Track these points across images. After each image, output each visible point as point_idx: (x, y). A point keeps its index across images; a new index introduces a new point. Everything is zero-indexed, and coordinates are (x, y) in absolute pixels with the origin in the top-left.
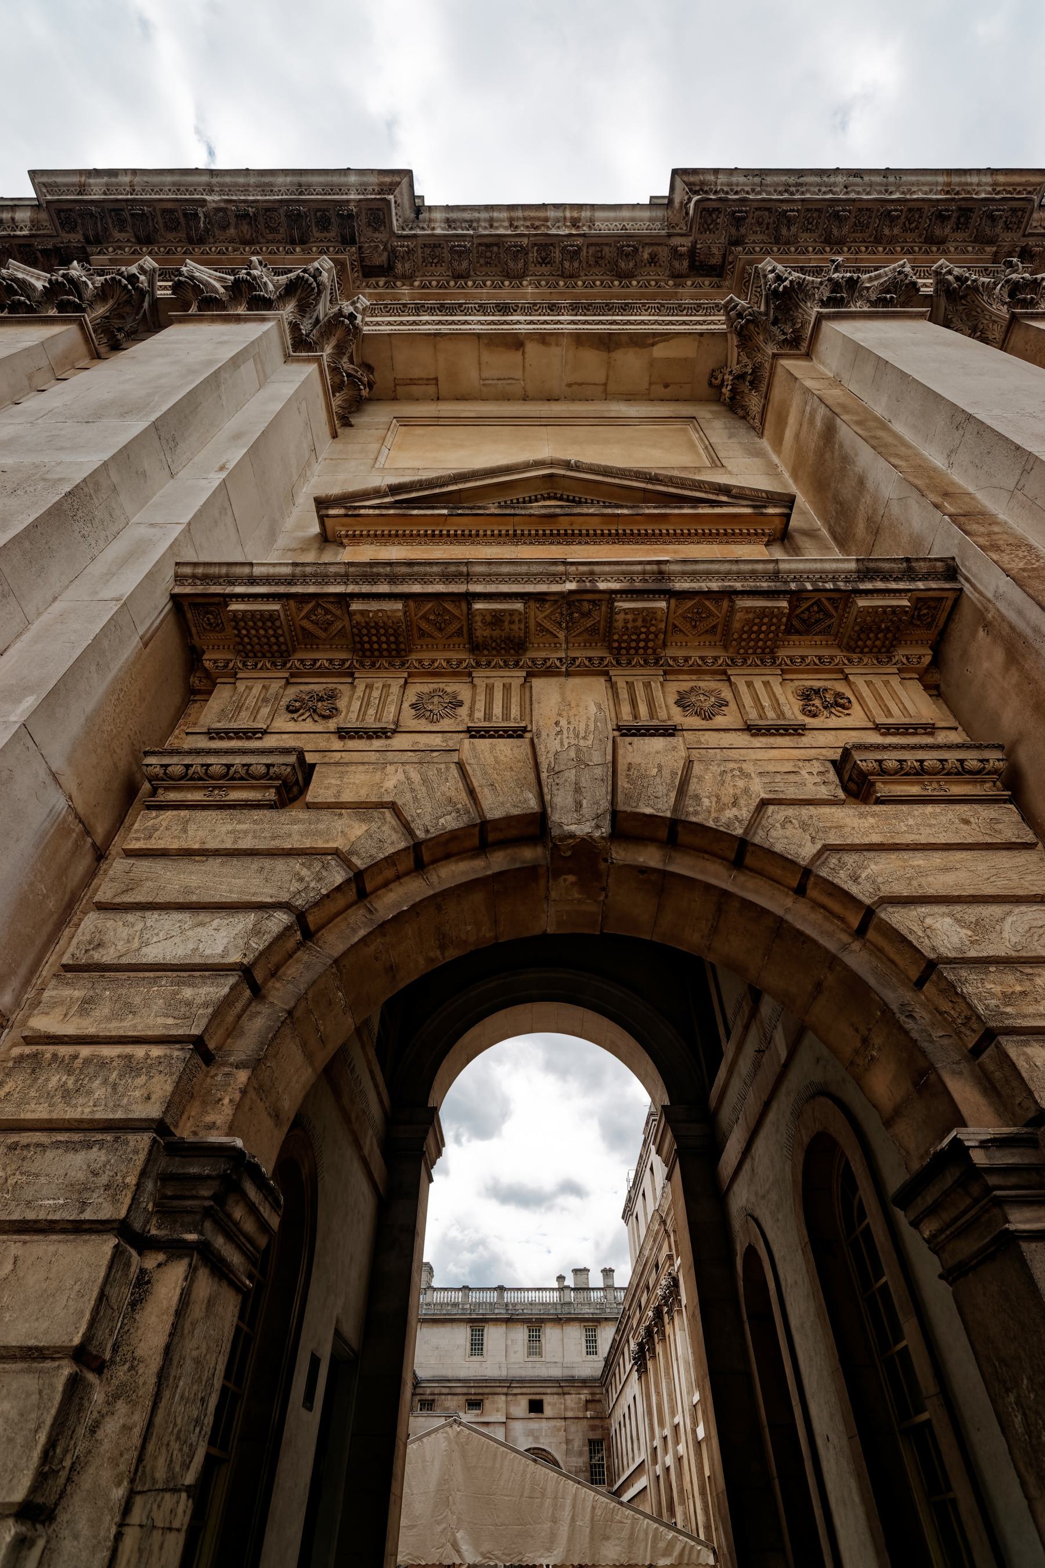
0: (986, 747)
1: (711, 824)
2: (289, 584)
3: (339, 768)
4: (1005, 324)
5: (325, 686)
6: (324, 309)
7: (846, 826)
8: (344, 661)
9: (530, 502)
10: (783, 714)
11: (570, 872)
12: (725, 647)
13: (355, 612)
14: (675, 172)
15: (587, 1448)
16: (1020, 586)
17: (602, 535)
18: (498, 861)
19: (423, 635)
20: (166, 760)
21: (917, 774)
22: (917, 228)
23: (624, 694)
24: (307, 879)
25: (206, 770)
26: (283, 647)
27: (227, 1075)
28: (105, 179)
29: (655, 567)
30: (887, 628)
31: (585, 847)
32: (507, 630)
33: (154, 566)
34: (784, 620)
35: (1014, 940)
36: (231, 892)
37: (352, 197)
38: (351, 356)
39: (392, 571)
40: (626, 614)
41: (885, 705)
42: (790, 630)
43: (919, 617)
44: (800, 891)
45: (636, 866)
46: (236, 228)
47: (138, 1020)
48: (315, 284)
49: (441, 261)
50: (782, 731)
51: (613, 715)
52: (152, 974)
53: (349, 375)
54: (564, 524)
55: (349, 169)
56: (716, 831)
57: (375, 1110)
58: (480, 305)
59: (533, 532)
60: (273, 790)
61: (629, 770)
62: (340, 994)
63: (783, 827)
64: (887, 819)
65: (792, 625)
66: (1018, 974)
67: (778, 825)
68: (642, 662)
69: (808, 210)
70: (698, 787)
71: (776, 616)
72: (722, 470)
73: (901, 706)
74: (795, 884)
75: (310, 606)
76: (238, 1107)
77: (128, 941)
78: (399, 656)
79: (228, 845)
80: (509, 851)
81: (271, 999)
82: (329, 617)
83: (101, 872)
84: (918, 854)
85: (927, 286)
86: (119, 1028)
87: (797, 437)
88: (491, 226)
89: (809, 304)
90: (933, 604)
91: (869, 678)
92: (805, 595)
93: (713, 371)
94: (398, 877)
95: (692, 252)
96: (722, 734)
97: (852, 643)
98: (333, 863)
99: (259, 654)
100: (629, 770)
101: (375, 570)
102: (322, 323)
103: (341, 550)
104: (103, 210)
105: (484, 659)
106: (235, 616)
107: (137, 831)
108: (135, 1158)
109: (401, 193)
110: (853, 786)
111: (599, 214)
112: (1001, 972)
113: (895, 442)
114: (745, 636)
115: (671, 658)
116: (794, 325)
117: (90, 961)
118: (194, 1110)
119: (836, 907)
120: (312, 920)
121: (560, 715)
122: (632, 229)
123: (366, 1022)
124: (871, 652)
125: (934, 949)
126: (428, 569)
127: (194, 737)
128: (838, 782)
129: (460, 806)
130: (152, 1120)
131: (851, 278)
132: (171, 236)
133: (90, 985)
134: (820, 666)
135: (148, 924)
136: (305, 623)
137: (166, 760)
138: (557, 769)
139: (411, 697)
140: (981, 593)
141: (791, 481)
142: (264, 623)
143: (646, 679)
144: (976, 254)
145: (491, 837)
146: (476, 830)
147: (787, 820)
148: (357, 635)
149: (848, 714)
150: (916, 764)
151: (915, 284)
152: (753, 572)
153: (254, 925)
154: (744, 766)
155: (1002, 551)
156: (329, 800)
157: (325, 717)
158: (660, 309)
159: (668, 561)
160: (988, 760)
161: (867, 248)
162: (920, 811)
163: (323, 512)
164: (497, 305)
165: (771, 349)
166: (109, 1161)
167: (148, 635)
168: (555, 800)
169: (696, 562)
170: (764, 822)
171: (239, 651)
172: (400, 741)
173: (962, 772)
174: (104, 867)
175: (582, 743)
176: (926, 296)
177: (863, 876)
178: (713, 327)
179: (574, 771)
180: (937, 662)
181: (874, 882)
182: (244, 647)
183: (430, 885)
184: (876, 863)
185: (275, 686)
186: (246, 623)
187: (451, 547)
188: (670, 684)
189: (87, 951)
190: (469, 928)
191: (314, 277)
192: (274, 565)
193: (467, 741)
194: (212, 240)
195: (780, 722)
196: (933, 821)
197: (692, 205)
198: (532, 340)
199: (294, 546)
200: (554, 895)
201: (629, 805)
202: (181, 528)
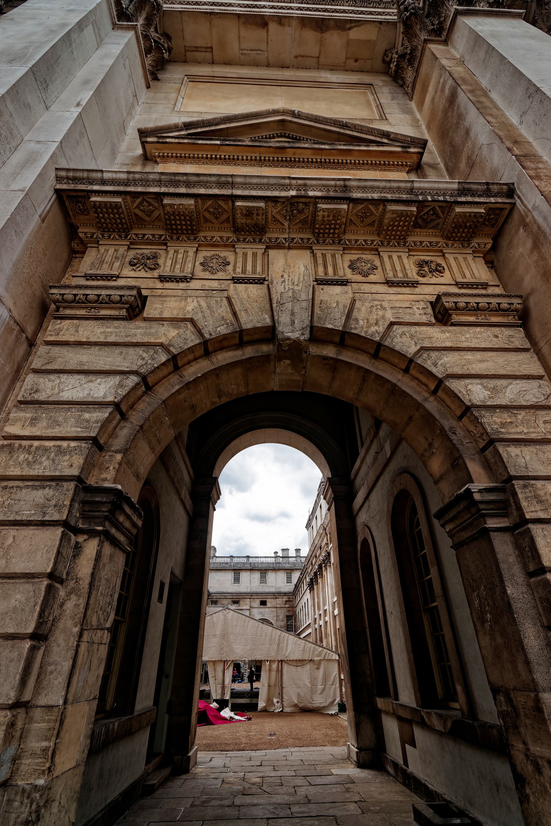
0: (513, 296)
1: (363, 334)
2: (126, 185)
3: (161, 299)
5: (151, 250)
8: (161, 236)
10: (407, 274)
12: (379, 235)
13: (167, 205)
18: (249, 352)
19: (207, 222)
20: (63, 291)
21: (475, 310)
23: (320, 261)
24: (146, 359)
30: (470, 226)
31: (296, 343)
32: (255, 219)
34: (413, 218)
35: (511, 397)
36: (105, 365)
40: (324, 212)
41: (463, 272)
42: (416, 225)
44: (406, 371)
45: (322, 356)
50: (405, 285)
52: (67, 406)
60: (124, 310)
62: (167, 418)
63: (401, 337)
64: (455, 334)
65: (417, 222)
66: (510, 413)
67: (398, 336)
68: (331, 242)
74: (404, 367)
76: (118, 471)
77: (52, 389)
79: (102, 339)
80: (255, 347)
82: (151, 207)
83: (33, 353)
84: (469, 353)
90: (497, 212)
91: (455, 255)
92: (427, 204)
94: (195, 359)
96: (373, 285)
97: (449, 235)
98: (160, 350)
99: (111, 230)
101: (177, 178)
107: (50, 331)
110: (440, 316)
113: (491, 106)
114: (390, 228)
115: (348, 240)
116: (440, 18)
118: (96, 472)
119: (424, 379)
120: (150, 380)
121: (284, 271)
124: (459, 240)
125: (470, 401)
126: (209, 179)
127: (78, 278)
128: (432, 314)
129: (228, 321)
130: (75, 476)
133: (34, 411)
134: (431, 248)
136: (137, 211)
137: (63, 291)
138: (282, 302)
139: (200, 259)
140: (525, 206)
142: (112, 210)
143: (333, 252)
145: (246, 338)
146: (237, 335)
147: (403, 333)
148: (168, 220)
149: (442, 276)
152: (399, 188)
154: (383, 303)
155: (542, 180)
156: (156, 316)
157: (151, 269)
159: (350, 179)
160: (513, 304)
162: (474, 330)
165: (423, 36)
166: (55, 494)
168: (280, 319)
169: (366, 180)
170: (391, 334)
172: (194, 284)
173: (499, 310)
175: (296, 288)
177: (440, 363)
179: (291, 303)
180: (495, 248)
182: (102, 225)
183: (213, 363)
184: (447, 357)
185: (122, 250)
186: (102, 210)
189: (30, 394)
190: (233, 387)
192: (116, 172)
193: (232, 285)
195: (405, 279)
196: (479, 336)
200: (278, 370)
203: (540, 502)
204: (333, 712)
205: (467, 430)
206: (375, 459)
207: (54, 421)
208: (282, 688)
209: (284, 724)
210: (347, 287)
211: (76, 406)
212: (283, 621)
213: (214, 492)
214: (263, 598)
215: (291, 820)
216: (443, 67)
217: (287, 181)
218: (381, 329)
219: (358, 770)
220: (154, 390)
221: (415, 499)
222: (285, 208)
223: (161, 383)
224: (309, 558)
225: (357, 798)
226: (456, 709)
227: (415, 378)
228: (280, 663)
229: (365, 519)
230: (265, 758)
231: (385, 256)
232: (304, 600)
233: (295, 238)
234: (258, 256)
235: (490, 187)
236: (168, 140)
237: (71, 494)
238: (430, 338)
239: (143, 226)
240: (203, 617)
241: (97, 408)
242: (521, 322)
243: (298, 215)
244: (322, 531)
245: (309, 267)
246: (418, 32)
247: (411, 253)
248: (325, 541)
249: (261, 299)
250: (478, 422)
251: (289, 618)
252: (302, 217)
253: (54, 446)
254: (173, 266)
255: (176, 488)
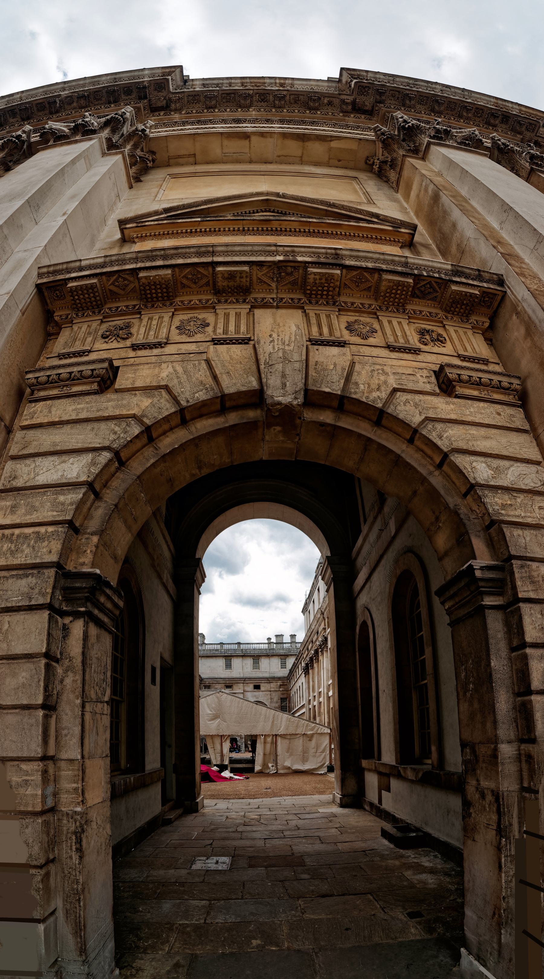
0: (513, 377)
1: (364, 400)
2: (102, 267)
3: (134, 368)
4: (528, 171)
5: (124, 321)
6: (126, 129)
7: (438, 408)
8: (135, 306)
9: (254, 213)
10: (408, 341)
11: (277, 425)
12: (376, 300)
13: (142, 278)
14: (342, 69)
15: (280, 701)
16: (535, 298)
17: (300, 231)
18: (233, 418)
19: (184, 287)
20: (37, 375)
21: (477, 385)
22: (481, 116)
23: (313, 320)
24: (118, 432)
25: (59, 377)
26: (99, 302)
27: (87, 539)
28: (7, 99)
29: (333, 251)
30: (467, 304)
32: (238, 282)
33: (27, 272)
34: (411, 289)
36: (77, 443)
37: (146, 79)
38: (143, 148)
39: (164, 253)
40: (315, 275)
41: (464, 345)
42: (414, 295)
43: (484, 301)
44: (411, 441)
45: (318, 422)
46: (77, 102)
47: (39, 514)
48: (122, 119)
49: (199, 101)
50: (407, 351)
51: (307, 332)
52: (42, 490)
53: (140, 157)
54: (275, 225)
55: (144, 69)
56: (367, 404)
57: (167, 554)
58: (223, 120)
59: (255, 229)
60: (96, 384)
61: (316, 365)
62: (142, 495)
63: (405, 405)
64: (460, 406)
65: (415, 293)
66: (510, 496)
67: (402, 403)
68: (325, 303)
69: (421, 96)
70: (357, 378)
71: (406, 287)
72: (374, 206)
73: (472, 347)
74: (408, 437)
75: (115, 277)
76: (95, 554)
77: (28, 474)
78: (169, 299)
79: (74, 417)
80: (240, 412)
81: (105, 499)
82: (126, 282)
83: (11, 440)
84: (474, 428)
85: (488, 143)
86: (31, 519)
87: (418, 196)
88: (230, 86)
89: (423, 136)
90: (491, 296)
91: (456, 328)
92: (422, 278)
93: (368, 157)
95: (354, 103)
96: (373, 349)
97: (448, 308)
98: (133, 422)
99: (85, 308)
100: (316, 365)
101: (154, 253)
102: (125, 136)
103: (134, 245)
104: (5, 112)
105: (223, 298)
106: (71, 289)
107: (26, 415)
108: (49, 580)
109: (175, 75)
110: (444, 386)
111: (296, 82)
112: (503, 493)
113: (472, 210)
114: (388, 295)
115: (343, 302)
116: (415, 143)
117: (12, 487)
118: (73, 556)
119: (429, 451)
120: (123, 455)
121: (273, 331)
122: (316, 89)
123: (158, 509)
124: (458, 315)
125: (475, 478)
126: (188, 250)
127: (51, 359)
128: (436, 383)
130: (54, 562)
131: (446, 130)
132: (40, 114)
133: (14, 499)
134: (430, 318)
135: (37, 464)
136: (112, 288)
137: (37, 375)
138: (270, 363)
139: (176, 322)
140: (515, 296)
141: (414, 218)
142: (88, 291)
143: (328, 313)
144: (512, 136)
147: (407, 402)
148: (143, 290)
149: (444, 347)
150: (478, 379)
151: (481, 140)
152: (393, 261)
153: (92, 460)
154: (385, 368)
155: (527, 278)
156: (128, 387)
157: (124, 339)
158: (334, 125)
159: (341, 249)
160: (512, 384)
161: (454, 119)
162: (477, 405)
163: (123, 227)
164: (233, 120)
165: (401, 152)
166: (37, 583)
167: (24, 309)
168: (269, 382)
169: (359, 251)
170: (394, 401)
171: (74, 308)
173: (499, 388)
174: (12, 437)
175: (287, 348)
176: (487, 147)
178: (367, 137)
179: (281, 365)
180: (492, 327)
181: (450, 440)
182: (77, 305)
184: (452, 430)
185: (95, 325)
186: (77, 292)
187: (203, 238)
188: (342, 316)
189: (9, 481)
190: (215, 457)
191: (122, 116)
192: (93, 258)
194: (63, 110)
195: (406, 345)
197: (353, 83)
198: (255, 135)
199: (105, 246)
200: (267, 438)
201: (316, 386)
202: (41, 249)
203: (533, 582)
204: (323, 772)
205: (471, 509)
206: (379, 537)
207: (32, 506)
208: (277, 756)
209: (279, 781)
210: (345, 348)
211: (51, 489)
212: (277, 702)
213: (198, 574)
214: (256, 683)
215: (284, 839)
216: (423, 175)
217: (274, 248)
218: (384, 395)
219: (341, 809)
220: (128, 466)
221: (417, 580)
222: (272, 271)
223: (134, 457)
224: (305, 643)
225: (338, 826)
226: (428, 764)
227: (419, 450)
228: (274, 737)
229: (366, 601)
230: (262, 803)
231: (385, 321)
232: (299, 683)
233: (284, 298)
234: (242, 315)
235: (482, 273)
236: (147, 224)
237: (52, 581)
238: (435, 408)
239: (117, 300)
240: (197, 698)
241: (71, 490)
242: (521, 403)
243: (287, 277)
244: (319, 616)
245: (301, 326)
246: (397, 149)
247: (411, 321)
248: (322, 626)
249: (246, 360)
250: (481, 502)
251: (283, 700)
252: (291, 279)
253: (33, 533)
254: (147, 333)
255: (156, 571)
